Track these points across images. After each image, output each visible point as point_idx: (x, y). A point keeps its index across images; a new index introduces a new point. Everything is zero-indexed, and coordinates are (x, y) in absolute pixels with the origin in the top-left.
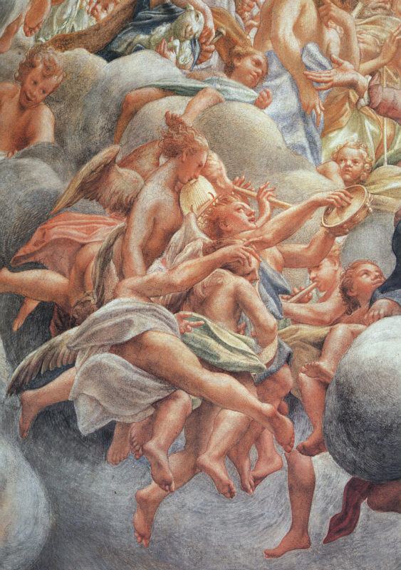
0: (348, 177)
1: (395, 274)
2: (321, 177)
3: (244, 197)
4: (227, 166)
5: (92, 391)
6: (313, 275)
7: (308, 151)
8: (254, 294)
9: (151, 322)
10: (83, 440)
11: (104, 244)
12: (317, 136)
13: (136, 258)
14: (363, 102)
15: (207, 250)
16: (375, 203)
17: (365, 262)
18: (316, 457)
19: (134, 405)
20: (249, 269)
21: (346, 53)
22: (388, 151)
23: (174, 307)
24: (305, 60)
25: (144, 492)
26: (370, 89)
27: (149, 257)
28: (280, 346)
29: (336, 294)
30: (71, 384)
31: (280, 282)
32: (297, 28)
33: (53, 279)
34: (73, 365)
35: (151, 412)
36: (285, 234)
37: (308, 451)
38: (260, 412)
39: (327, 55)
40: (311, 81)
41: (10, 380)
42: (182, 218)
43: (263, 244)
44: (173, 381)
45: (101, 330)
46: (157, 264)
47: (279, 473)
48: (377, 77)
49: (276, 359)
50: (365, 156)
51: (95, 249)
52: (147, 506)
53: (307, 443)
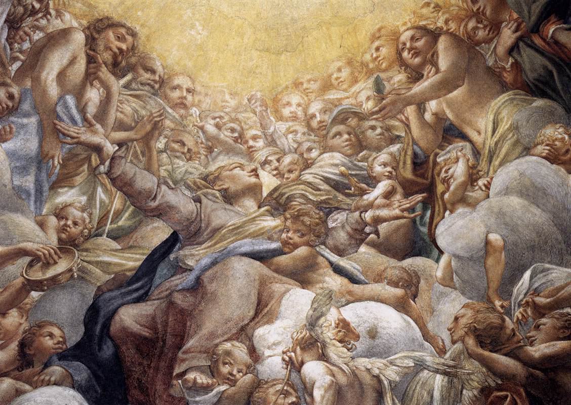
0: (64, 236)
1: (78, 346)
2: (37, 228)
7: (33, 198)
12: (46, 187)
14: (102, 169)
17: (52, 324)
21: (102, 115)
22: (110, 224)
24: (59, 109)
32: (61, 76)
39: (82, 111)
40: (57, 132)
48: (123, 149)
50: (87, 221)
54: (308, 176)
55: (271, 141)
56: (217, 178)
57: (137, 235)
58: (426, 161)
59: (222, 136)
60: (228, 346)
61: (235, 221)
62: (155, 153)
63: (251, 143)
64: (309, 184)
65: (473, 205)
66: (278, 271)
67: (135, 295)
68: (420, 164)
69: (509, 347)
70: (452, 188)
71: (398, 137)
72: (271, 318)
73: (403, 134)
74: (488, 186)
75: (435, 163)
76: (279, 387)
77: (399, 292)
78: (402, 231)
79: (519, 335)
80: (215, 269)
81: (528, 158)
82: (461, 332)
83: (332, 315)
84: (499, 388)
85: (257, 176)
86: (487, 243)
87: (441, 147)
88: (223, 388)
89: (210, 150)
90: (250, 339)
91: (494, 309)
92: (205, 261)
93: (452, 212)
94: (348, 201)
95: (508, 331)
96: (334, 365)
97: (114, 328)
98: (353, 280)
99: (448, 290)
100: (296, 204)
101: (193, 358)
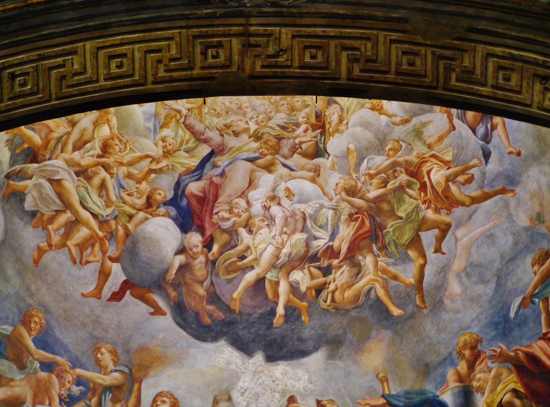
0: (165, 150)
1: (172, 199)
2: (154, 146)
3: (120, 141)
4: (118, 124)
5: (35, 193)
6: (137, 185)
7: (152, 132)
8: (111, 183)
9: (66, 176)
10: (24, 211)
11: (60, 135)
13: (70, 147)
14: (182, 120)
15: (99, 156)
16: (173, 165)
17: (160, 189)
18: (114, 264)
19: (49, 208)
20: (112, 172)
23: (78, 174)
25: (41, 245)
26: (186, 116)
27: (76, 148)
28: (114, 210)
29: (144, 199)
30: (27, 187)
31: (123, 183)
33: (37, 140)
34: (31, 178)
35: (54, 213)
36: (131, 164)
37: (112, 260)
38: (97, 234)
41: (7, 172)
42: (93, 138)
43: (121, 164)
44: (67, 206)
45: (47, 170)
46: (77, 153)
47: (97, 263)
48: (190, 112)
49: (110, 216)
51: (56, 135)
52: (41, 251)
53: (113, 256)
54: (270, 124)
55: (254, 109)
56: (230, 126)
57: (196, 151)
58: (321, 115)
59: (232, 107)
60: (237, 200)
61: (240, 144)
62: (203, 114)
63: (245, 110)
64: (271, 128)
65: (341, 132)
66: (258, 166)
67: (196, 178)
68: (318, 116)
69: (359, 195)
70: (332, 126)
71: (308, 105)
72: (255, 188)
73: (311, 103)
74: (347, 124)
75: (325, 115)
76: (260, 218)
77: (312, 174)
78: (312, 147)
79: (364, 189)
80: (231, 166)
81: (363, 109)
82: (339, 190)
83: (283, 186)
84: (356, 213)
85: (248, 124)
86: (348, 149)
87: (327, 108)
88: (235, 219)
89: (227, 113)
90: (247, 197)
91: (353, 179)
92: (226, 163)
93: (333, 136)
94: (288, 134)
95: (359, 188)
96: (284, 207)
97: (187, 191)
98: (292, 170)
99: (333, 171)
100: (265, 137)
101: (221, 206)
